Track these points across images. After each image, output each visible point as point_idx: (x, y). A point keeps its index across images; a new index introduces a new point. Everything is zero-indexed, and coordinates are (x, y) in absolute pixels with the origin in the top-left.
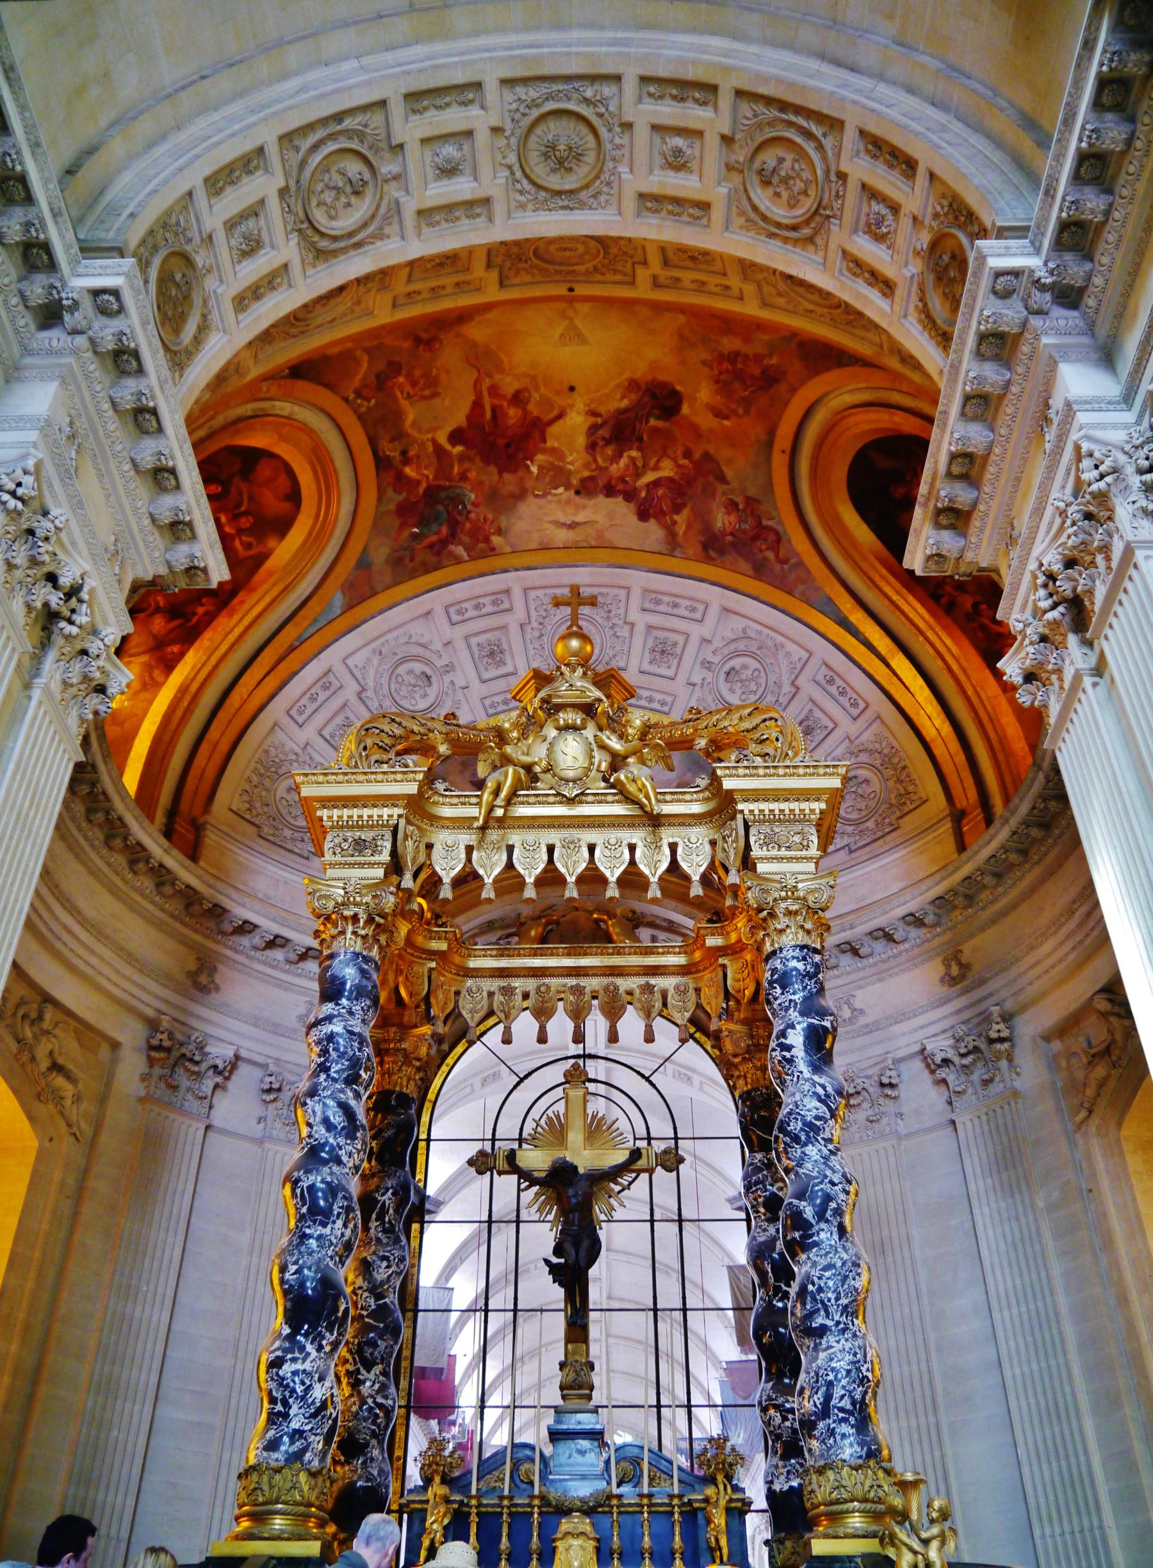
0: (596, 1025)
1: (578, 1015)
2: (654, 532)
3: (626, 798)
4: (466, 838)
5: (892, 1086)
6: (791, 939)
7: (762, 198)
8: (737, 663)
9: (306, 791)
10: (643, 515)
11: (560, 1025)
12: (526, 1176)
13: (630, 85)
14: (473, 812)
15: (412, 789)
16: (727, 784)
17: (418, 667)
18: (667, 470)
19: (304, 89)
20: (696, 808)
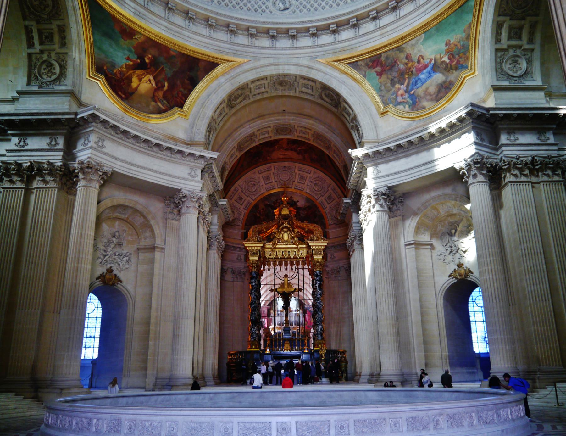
0: (289, 267)
1: (286, 265)
2: (300, 157)
3: (294, 244)
4: (269, 250)
5: (339, 272)
6: (318, 269)
7: (320, 142)
8: (317, 182)
9: (246, 245)
10: (298, 154)
11: (283, 267)
12: (279, 293)
13: (296, 127)
14: (271, 246)
15: (262, 245)
16: (310, 244)
17: (252, 183)
18: (303, 148)
19: (240, 134)
20: (305, 246)
